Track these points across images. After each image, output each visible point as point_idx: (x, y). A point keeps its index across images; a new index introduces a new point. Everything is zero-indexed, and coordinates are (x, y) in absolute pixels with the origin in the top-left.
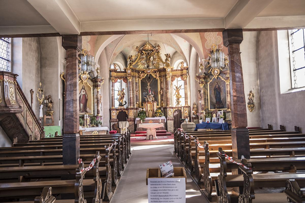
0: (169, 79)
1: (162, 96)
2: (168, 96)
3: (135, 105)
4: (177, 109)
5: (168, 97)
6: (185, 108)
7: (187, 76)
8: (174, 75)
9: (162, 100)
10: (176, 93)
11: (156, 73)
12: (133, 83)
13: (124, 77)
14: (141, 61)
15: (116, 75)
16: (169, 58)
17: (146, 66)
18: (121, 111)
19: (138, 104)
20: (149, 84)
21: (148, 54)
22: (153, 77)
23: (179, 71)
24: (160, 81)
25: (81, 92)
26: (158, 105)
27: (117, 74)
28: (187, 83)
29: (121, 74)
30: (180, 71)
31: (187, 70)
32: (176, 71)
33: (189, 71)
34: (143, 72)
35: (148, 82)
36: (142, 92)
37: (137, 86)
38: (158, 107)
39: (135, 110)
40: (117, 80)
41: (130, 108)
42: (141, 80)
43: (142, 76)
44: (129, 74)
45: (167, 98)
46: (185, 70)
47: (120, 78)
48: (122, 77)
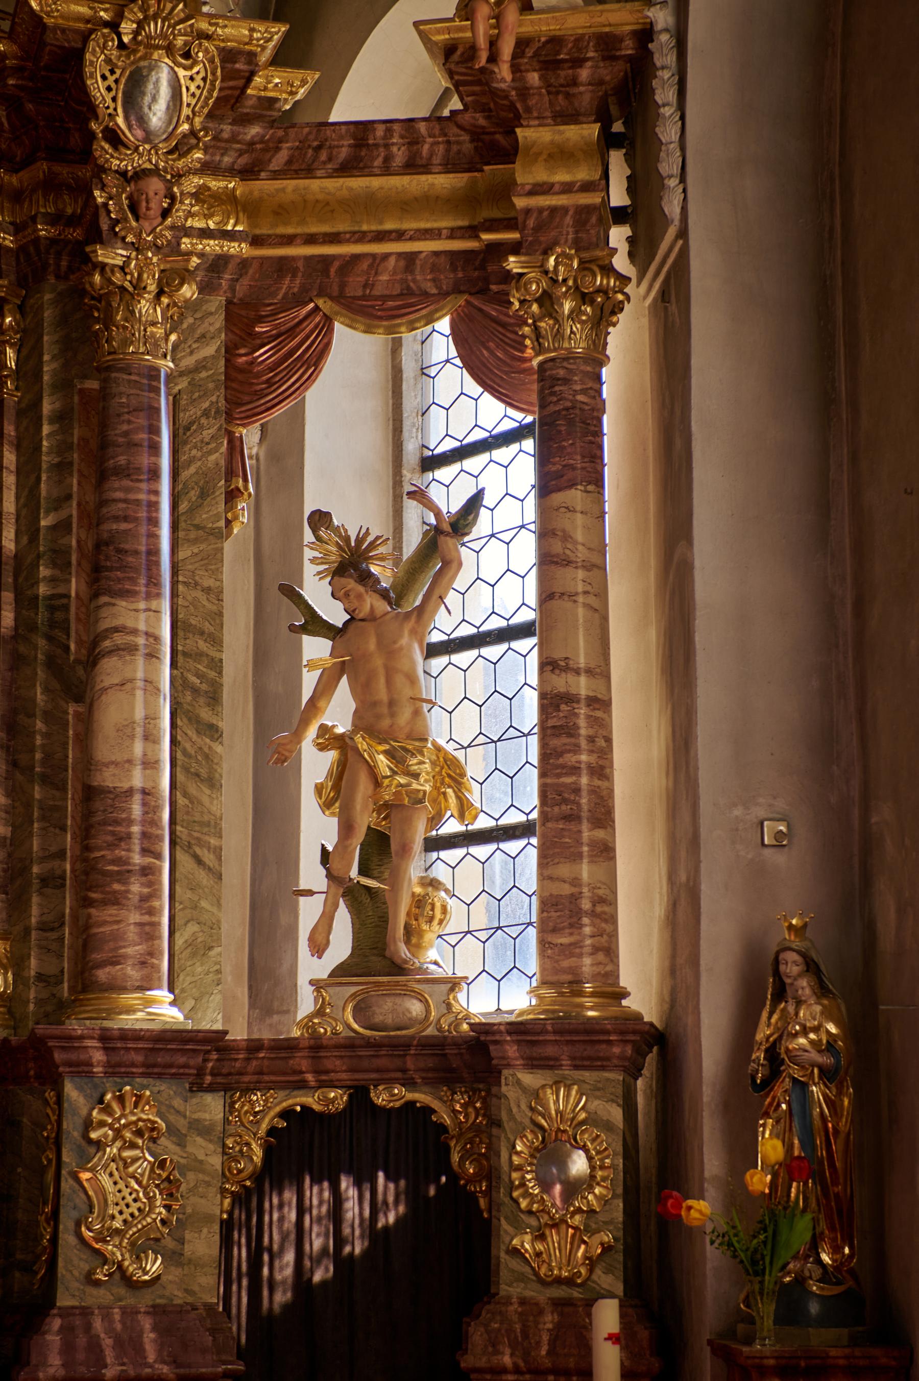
2: (103, 751)
4: (338, 1098)
5: (108, 778)
6: (529, 1079)
7: (625, 280)
23: (413, 166)
28: (595, 456)
30: (450, 167)
31: (617, 160)
32: (346, 169)
33: (669, 166)
46: (569, 117)
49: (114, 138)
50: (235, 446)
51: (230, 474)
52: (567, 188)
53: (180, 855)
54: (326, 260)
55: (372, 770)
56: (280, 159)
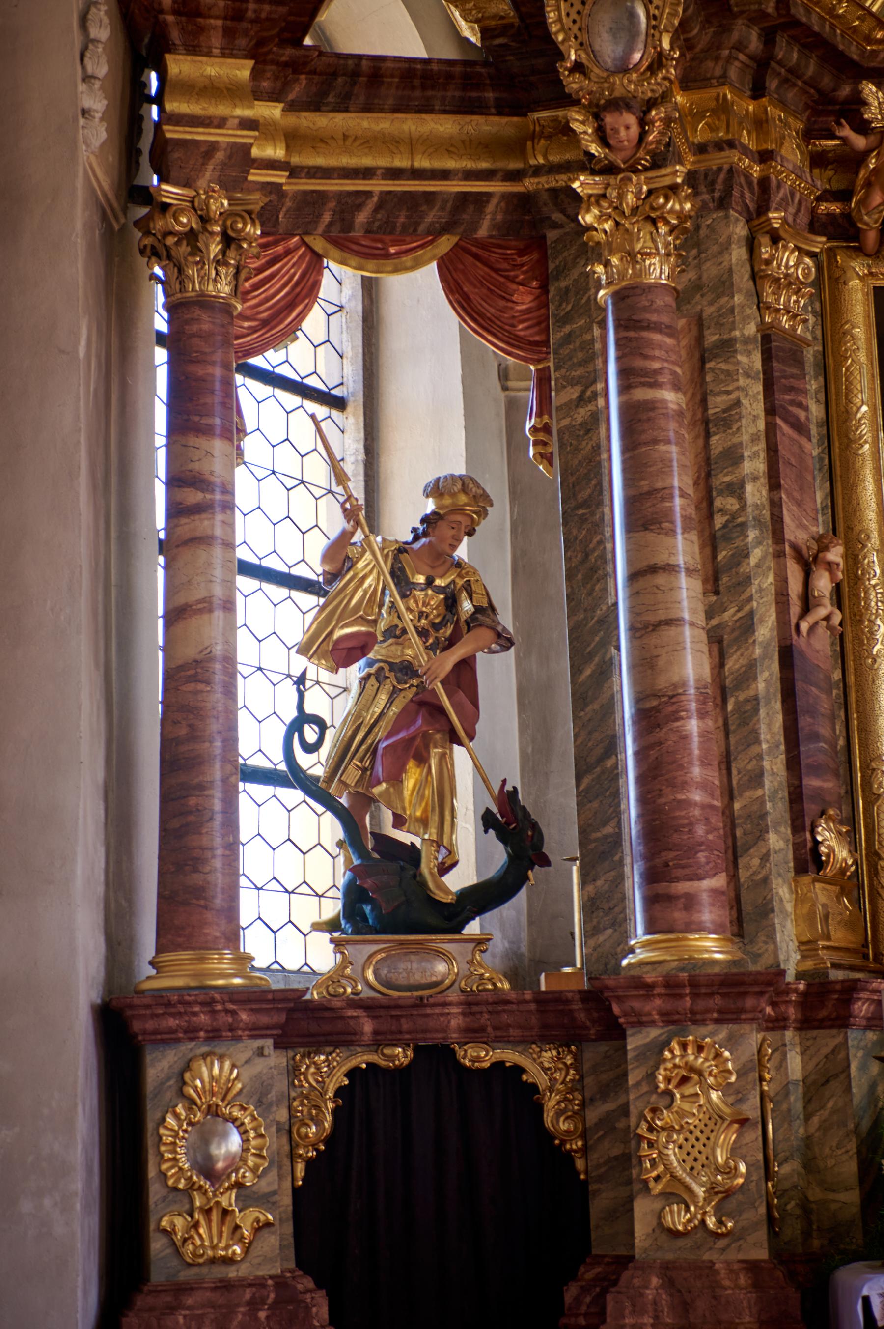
13: (481, 199)
15: (276, 152)
18: (401, 1055)
27: (292, 138)
29: (412, 144)
39: (777, 1024)
41: (672, 986)
44: (618, 104)
48: (411, 201)
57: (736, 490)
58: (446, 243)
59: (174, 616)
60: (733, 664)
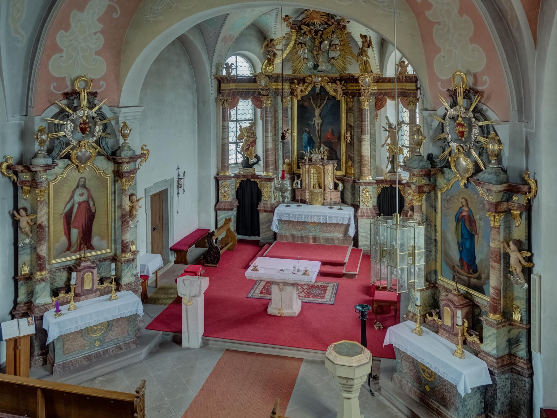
0: (367, 105)
1: (350, 145)
3: (281, 166)
8: (383, 91)
9: (350, 158)
10: (389, 141)
11: (336, 83)
12: (276, 111)
13: (255, 92)
14: (299, 52)
16: (369, 47)
17: (311, 64)
19: (289, 164)
20: (317, 112)
21: (316, 32)
22: (327, 93)
24: (347, 104)
25: (72, 197)
26: (339, 168)
27: (236, 86)
34: (302, 81)
35: (315, 107)
36: (300, 133)
37: (288, 117)
38: (339, 173)
40: (236, 99)
42: (298, 101)
43: (299, 91)
45: (362, 156)
47: (245, 95)
49: (362, 86)
50: (377, 113)
51: (376, 116)
52: (412, 90)
53: (372, 160)
54: (386, 92)
55: (392, 149)
56: (381, 81)
57: (278, 126)
58: (251, 97)
59: (223, 139)
60: (277, 143)
